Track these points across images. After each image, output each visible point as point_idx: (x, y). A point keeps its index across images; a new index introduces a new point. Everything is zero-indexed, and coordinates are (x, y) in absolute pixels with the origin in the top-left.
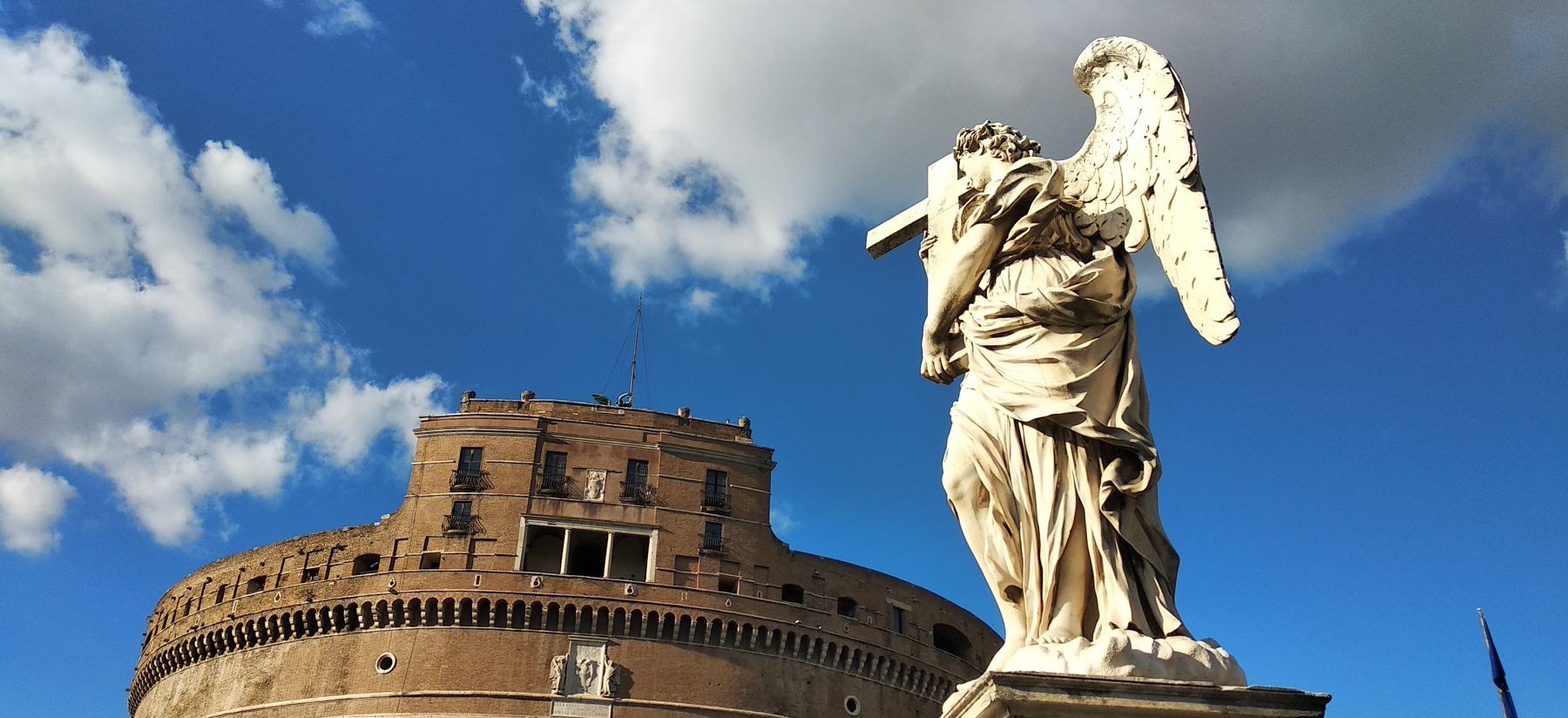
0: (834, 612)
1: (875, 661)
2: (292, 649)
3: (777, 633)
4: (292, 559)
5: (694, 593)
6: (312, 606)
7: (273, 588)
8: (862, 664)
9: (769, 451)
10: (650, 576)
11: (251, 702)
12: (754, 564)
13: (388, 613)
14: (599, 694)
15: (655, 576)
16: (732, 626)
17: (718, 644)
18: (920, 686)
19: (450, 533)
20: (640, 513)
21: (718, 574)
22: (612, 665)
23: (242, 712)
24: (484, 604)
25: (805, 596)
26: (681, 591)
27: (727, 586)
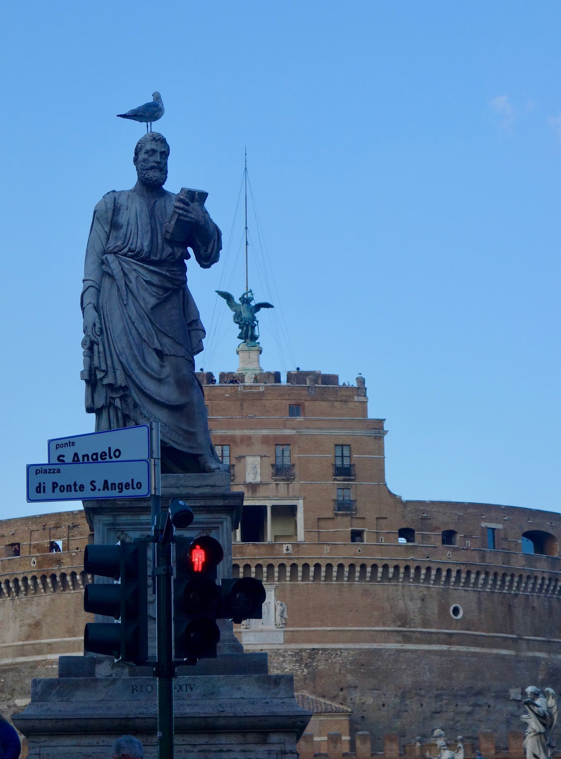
0: (439, 544)
1: (473, 576)
2: (53, 600)
3: (396, 568)
4: (38, 532)
5: (333, 546)
6: (63, 571)
7: (27, 554)
8: (463, 580)
9: (382, 421)
10: (301, 536)
11: (28, 638)
12: (377, 517)
14: (274, 626)
15: (305, 536)
16: (363, 567)
17: (354, 581)
20: (288, 488)
21: (350, 529)
22: (281, 605)
23: (23, 645)
25: (416, 536)
26: (324, 545)
27: (356, 535)
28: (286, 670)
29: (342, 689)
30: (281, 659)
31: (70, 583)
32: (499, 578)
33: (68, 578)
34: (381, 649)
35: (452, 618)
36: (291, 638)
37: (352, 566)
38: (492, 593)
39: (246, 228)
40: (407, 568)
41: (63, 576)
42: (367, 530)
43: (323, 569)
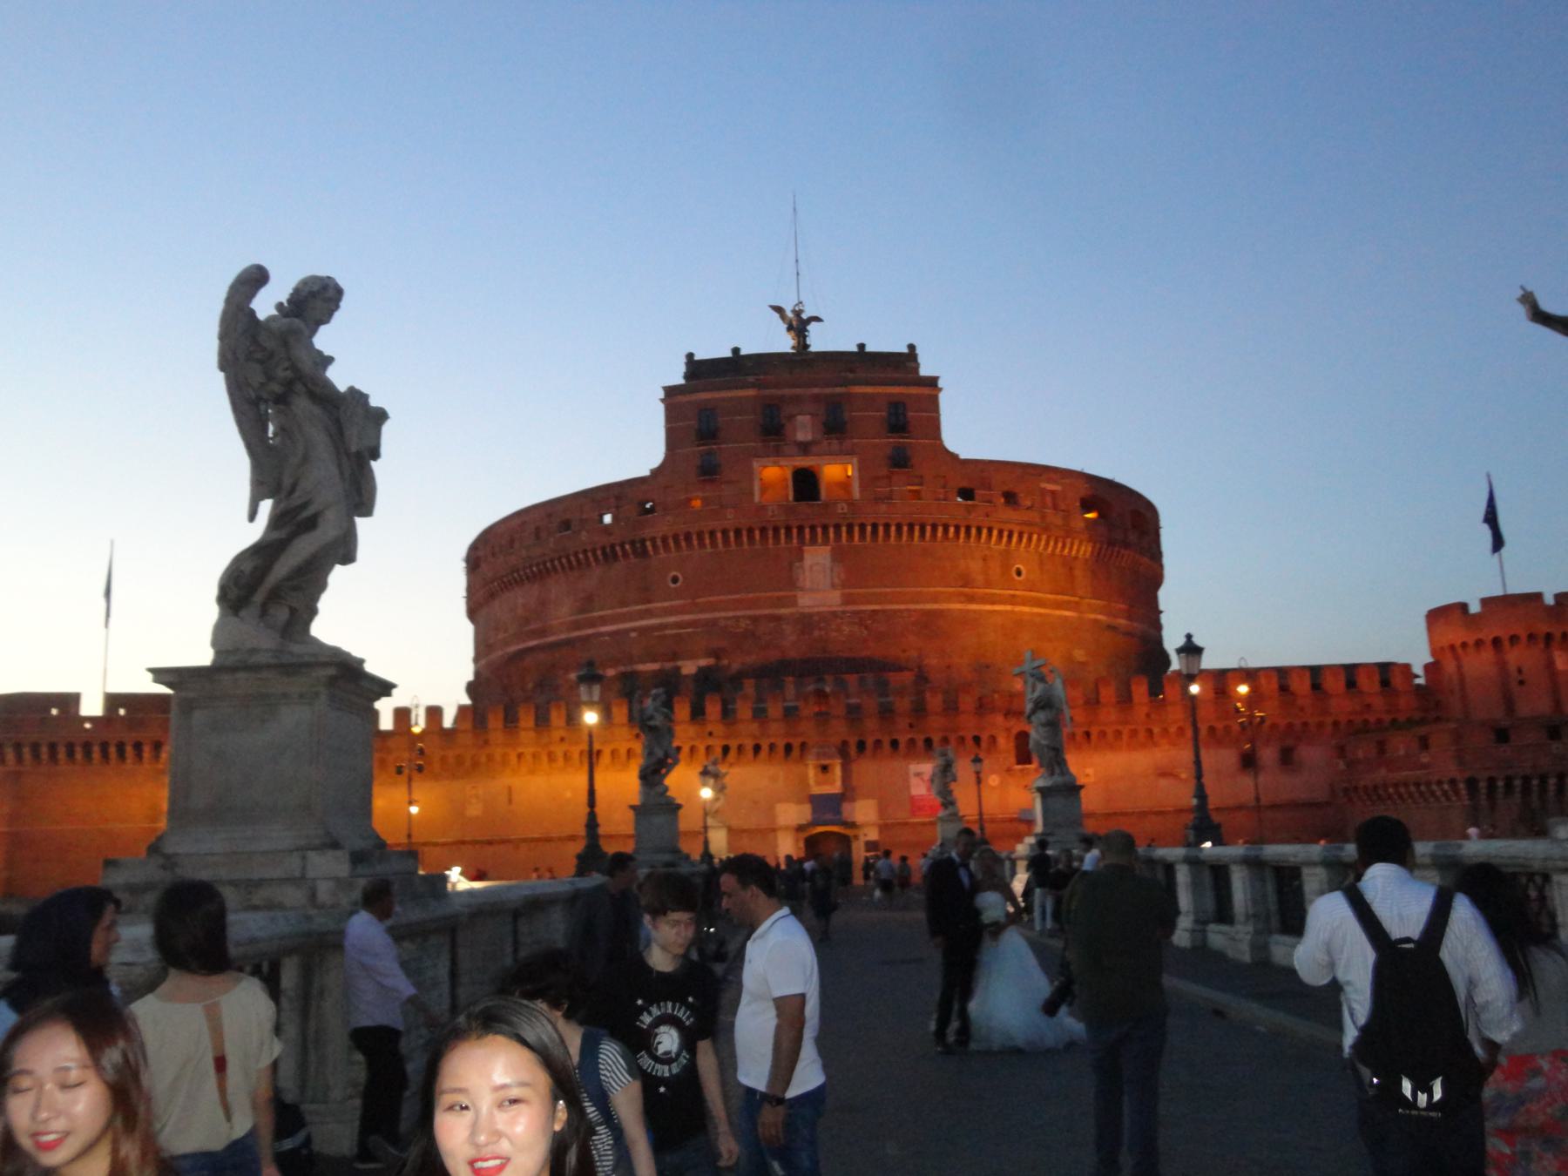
3: (957, 528)
10: (856, 493)
11: (582, 610)
13: (668, 544)
18: (1071, 549)
19: (704, 481)
24: (738, 532)
28: (845, 633)
29: (904, 651)
30: (839, 621)
31: (620, 553)
32: (1061, 540)
33: (618, 548)
34: (942, 611)
35: (1013, 579)
36: (848, 600)
37: (911, 527)
38: (1053, 553)
39: (797, 261)
40: (968, 529)
41: (612, 547)
42: (924, 488)
43: (881, 529)
